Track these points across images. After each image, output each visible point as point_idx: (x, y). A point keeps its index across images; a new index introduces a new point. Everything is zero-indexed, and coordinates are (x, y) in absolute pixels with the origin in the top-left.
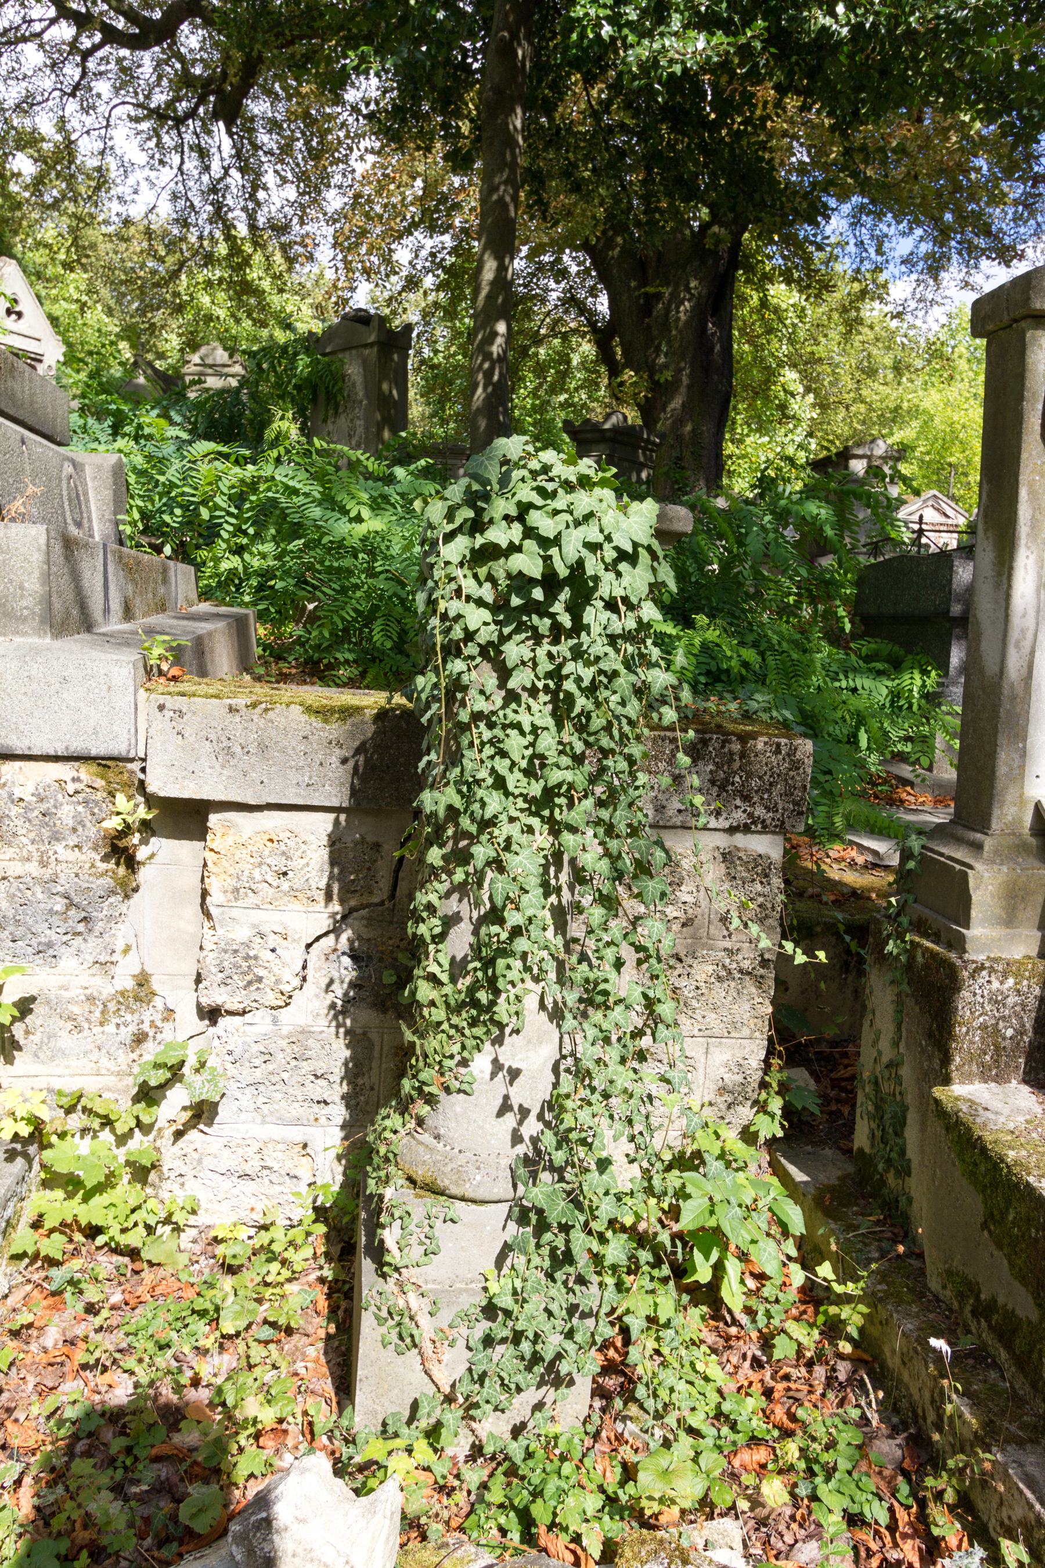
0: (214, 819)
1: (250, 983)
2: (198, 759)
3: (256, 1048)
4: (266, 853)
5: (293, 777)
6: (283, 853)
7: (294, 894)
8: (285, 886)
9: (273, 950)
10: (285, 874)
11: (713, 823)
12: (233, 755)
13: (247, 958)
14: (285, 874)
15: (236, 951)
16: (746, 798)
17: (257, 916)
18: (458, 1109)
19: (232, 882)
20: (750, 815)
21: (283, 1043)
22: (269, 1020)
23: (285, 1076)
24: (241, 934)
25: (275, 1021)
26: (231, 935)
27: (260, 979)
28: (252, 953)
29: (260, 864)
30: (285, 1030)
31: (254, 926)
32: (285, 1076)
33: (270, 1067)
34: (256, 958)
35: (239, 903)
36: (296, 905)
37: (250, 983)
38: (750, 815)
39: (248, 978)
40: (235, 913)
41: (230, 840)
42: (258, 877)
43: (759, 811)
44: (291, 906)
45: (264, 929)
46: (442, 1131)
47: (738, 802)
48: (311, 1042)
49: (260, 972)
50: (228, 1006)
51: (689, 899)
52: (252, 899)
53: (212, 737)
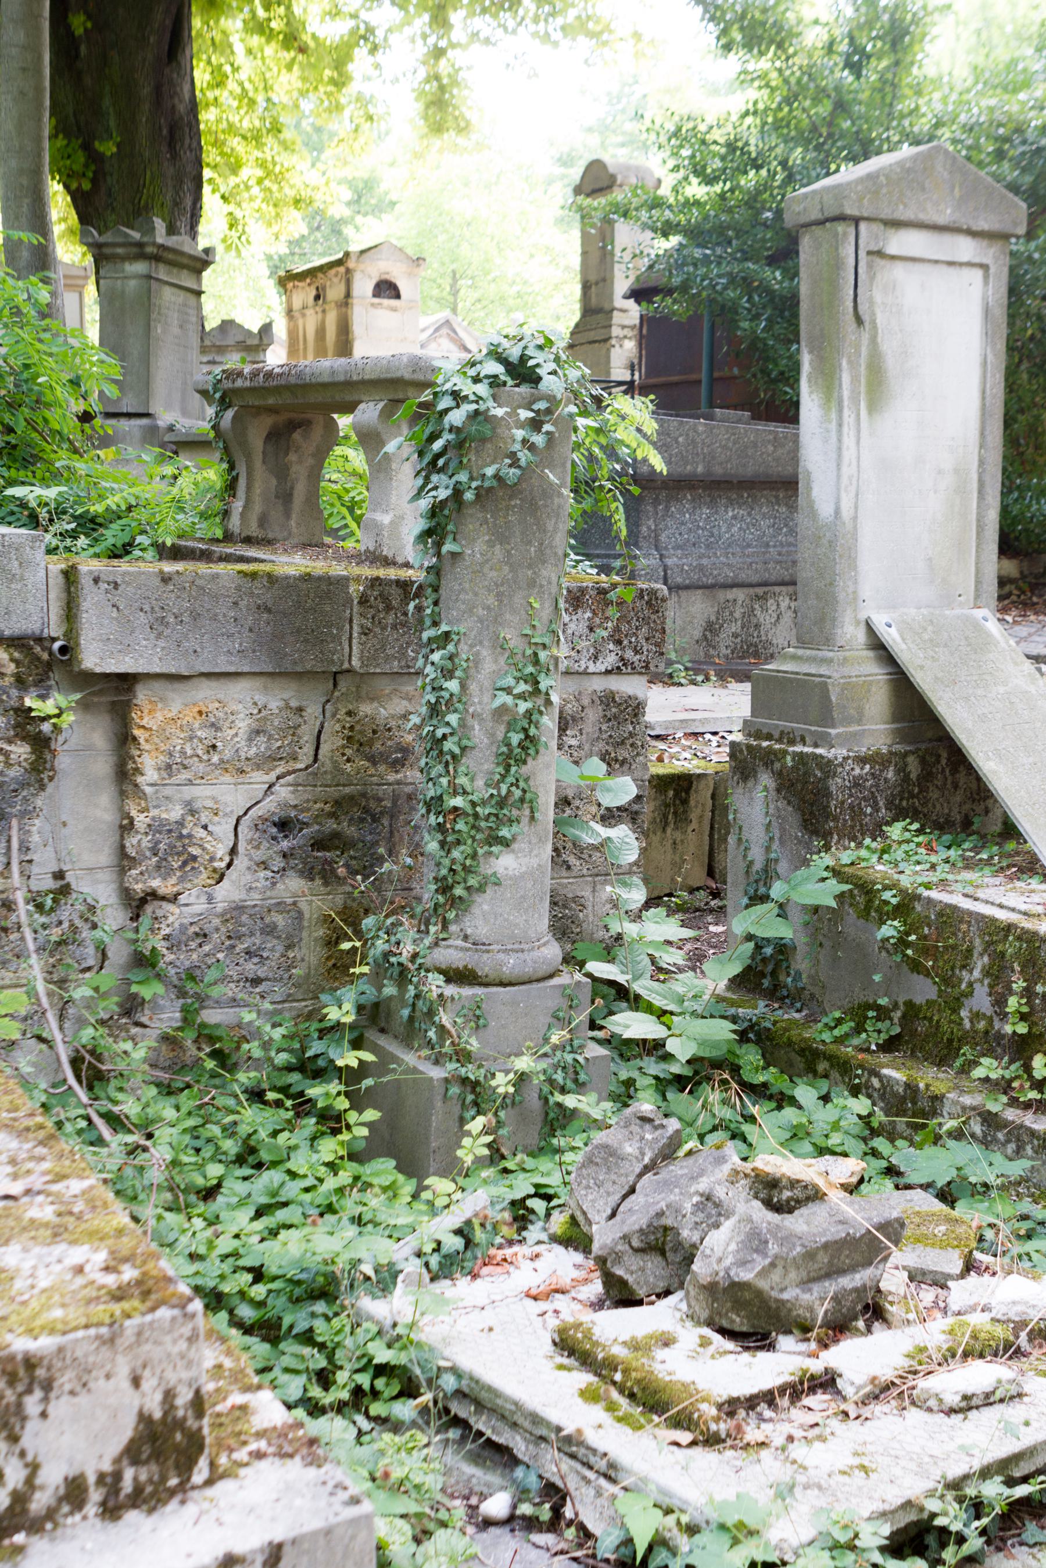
0: (142, 695)
1: (185, 863)
4: (196, 725)
6: (213, 725)
7: (224, 766)
8: (215, 759)
9: (205, 827)
11: (592, 668)
13: (181, 837)
15: (170, 831)
16: (619, 642)
17: (188, 792)
18: (486, 907)
19: (163, 759)
20: (622, 659)
21: (216, 922)
22: (203, 899)
23: (220, 956)
24: (175, 813)
25: (210, 899)
26: (164, 816)
27: (194, 858)
29: (191, 738)
30: (220, 907)
32: (220, 956)
33: (206, 948)
35: (173, 780)
36: (227, 778)
37: (185, 863)
38: (622, 659)
40: (168, 791)
41: (159, 716)
42: (189, 752)
43: (629, 654)
44: (222, 779)
45: (198, 805)
46: (469, 931)
47: (611, 646)
48: (244, 918)
49: (194, 851)
50: (162, 891)
51: (573, 742)
52: (185, 775)
53: (147, 607)
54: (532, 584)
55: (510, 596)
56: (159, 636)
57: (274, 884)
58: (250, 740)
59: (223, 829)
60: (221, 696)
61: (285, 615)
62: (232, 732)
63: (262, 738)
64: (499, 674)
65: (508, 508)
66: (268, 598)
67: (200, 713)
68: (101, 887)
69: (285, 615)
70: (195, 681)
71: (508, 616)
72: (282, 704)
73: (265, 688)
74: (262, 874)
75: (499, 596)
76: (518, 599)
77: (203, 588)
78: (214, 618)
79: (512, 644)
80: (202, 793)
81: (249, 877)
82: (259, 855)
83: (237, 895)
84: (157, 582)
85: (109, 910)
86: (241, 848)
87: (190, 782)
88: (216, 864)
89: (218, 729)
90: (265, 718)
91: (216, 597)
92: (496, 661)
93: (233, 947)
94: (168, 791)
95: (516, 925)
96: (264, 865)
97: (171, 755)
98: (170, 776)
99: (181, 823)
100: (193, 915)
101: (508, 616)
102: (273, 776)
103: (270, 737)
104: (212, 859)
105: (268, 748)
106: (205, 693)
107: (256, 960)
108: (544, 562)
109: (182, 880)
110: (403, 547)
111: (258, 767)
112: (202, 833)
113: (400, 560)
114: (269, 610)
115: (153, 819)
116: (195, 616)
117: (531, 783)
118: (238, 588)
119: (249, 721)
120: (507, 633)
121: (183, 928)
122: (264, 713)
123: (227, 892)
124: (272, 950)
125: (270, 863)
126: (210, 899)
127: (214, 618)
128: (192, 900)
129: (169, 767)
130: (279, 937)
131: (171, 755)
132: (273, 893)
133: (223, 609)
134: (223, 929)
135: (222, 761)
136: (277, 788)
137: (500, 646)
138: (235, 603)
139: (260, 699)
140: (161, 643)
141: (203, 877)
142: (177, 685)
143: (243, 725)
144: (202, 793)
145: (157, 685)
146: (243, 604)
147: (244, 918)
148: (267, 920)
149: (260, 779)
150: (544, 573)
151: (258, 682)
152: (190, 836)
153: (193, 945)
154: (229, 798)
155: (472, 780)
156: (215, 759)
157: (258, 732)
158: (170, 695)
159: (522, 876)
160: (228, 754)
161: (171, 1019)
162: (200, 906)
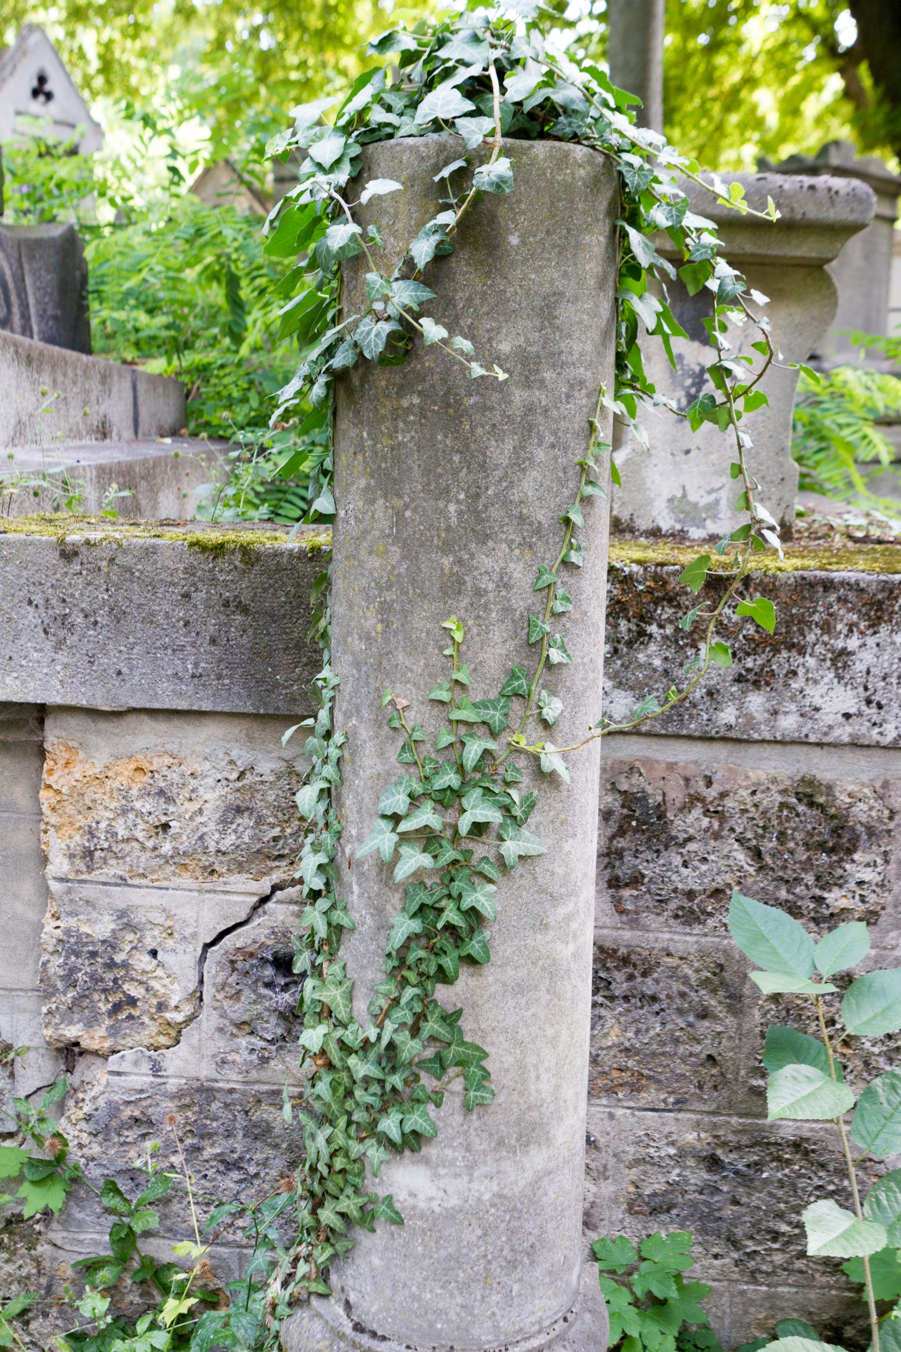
0: (54, 735)
1: (117, 1008)
2: (16, 637)
3: (127, 1112)
4: (134, 792)
5: (170, 664)
6: (161, 792)
7: (179, 861)
9: (154, 953)
10: (166, 827)
12: (71, 628)
13: (111, 965)
14: (166, 827)
15: (93, 954)
17: (123, 897)
19: (79, 840)
22: (146, 1067)
24: (101, 928)
25: (156, 1069)
26: (85, 929)
27: (132, 1002)
28: (119, 958)
29: (124, 812)
30: (173, 1085)
31: (122, 914)
34: (125, 965)
35: (95, 875)
36: (186, 880)
37: (117, 1008)
39: (113, 999)
40: (88, 891)
41: (77, 771)
42: (122, 833)
44: (177, 881)
45: (138, 918)
49: (135, 991)
51: (868, 875)
52: (113, 869)
53: (38, 599)
54: (452, 587)
55: (405, 614)
56: (59, 645)
57: (264, 1060)
58: (224, 822)
59: (181, 960)
60: (173, 747)
61: (273, 617)
62: (194, 806)
63: (245, 821)
64: (384, 781)
65: (396, 415)
66: (244, 589)
67: (139, 769)
68: (23, 1018)
69: (273, 617)
70: (132, 719)
71: (401, 657)
72: (280, 766)
73: (250, 738)
74: (243, 1042)
75: (385, 609)
76: (420, 621)
77: (129, 570)
78: (150, 619)
79: (411, 719)
80: (143, 900)
81: (221, 1044)
82: (238, 1010)
83: (206, 1071)
84: (53, 557)
85: (32, 1055)
86: (208, 991)
87: (123, 881)
88: (169, 1015)
89: (170, 800)
90: (252, 789)
91: (152, 586)
92: (382, 754)
93: (198, 1149)
94: (88, 891)
95: (439, 1313)
96: (246, 1026)
97: (92, 834)
98: (90, 869)
99: (111, 944)
100: (130, 1091)
101: (401, 657)
102: (264, 886)
103: (260, 821)
104: (161, 1007)
105: (255, 838)
106: (147, 737)
107: (236, 1175)
108: (483, 538)
109: (114, 1031)
110: (650, 502)
111: (241, 867)
112: (143, 961)
113: (643, 524)
114: (244, 610)
115: (68, 932)
116: (118, 615)
117: (466, 1024)
118: (190, 571)
119: (220, 791)
120: (400, 694)
121: (114, 1110)
122: (249, 779)
123: (185, 1063)
124: (265, 1163)
125: (259, 1025)
126: (156, 1069)
127: (150, 619)
128: (125, 1067)
129: (89, 854)
130: (276, 1146)
131: (92, 834)
132: (264, 1075)
133: (164, 605)
134: (180, 1119)
135: (176, 852)
136: (270, 905)
137: (388, 721)
138: (186, 596)
139: (243, 756)
140: (63, 657)
141: (150, 1031)
142: (103, 725)
143: (213, 797)
144: (143, 900)
145: (73, 722)
146: (199, 597)
147: (215, 1106)
148: (255, 1117)
149: (245, 887)
150: (486, 562)
151: (236, 729)
152: (125, 965)
153: (131, 1135)
154: (188, 913)
155: (350, 997)
156: (167, 848)
157: (239, 810)
158: (93, 739)
159: (450, 1216)
160: (185, 844)
161: (97, 1243)
162: (141, 1078)
